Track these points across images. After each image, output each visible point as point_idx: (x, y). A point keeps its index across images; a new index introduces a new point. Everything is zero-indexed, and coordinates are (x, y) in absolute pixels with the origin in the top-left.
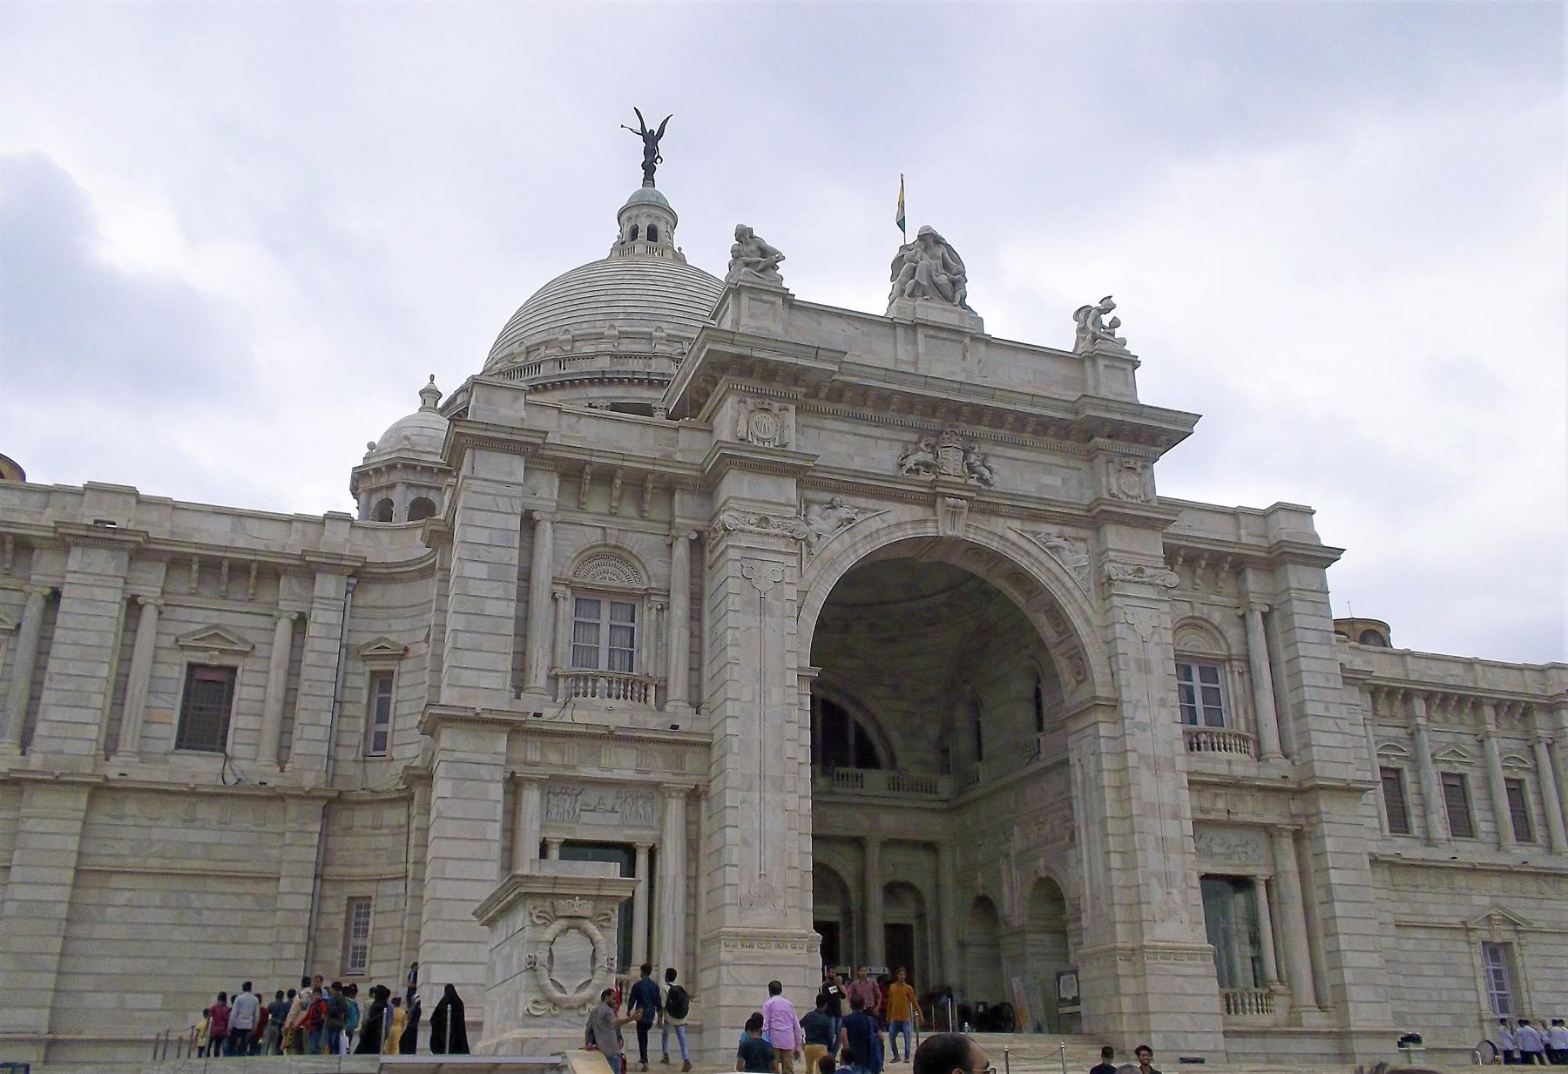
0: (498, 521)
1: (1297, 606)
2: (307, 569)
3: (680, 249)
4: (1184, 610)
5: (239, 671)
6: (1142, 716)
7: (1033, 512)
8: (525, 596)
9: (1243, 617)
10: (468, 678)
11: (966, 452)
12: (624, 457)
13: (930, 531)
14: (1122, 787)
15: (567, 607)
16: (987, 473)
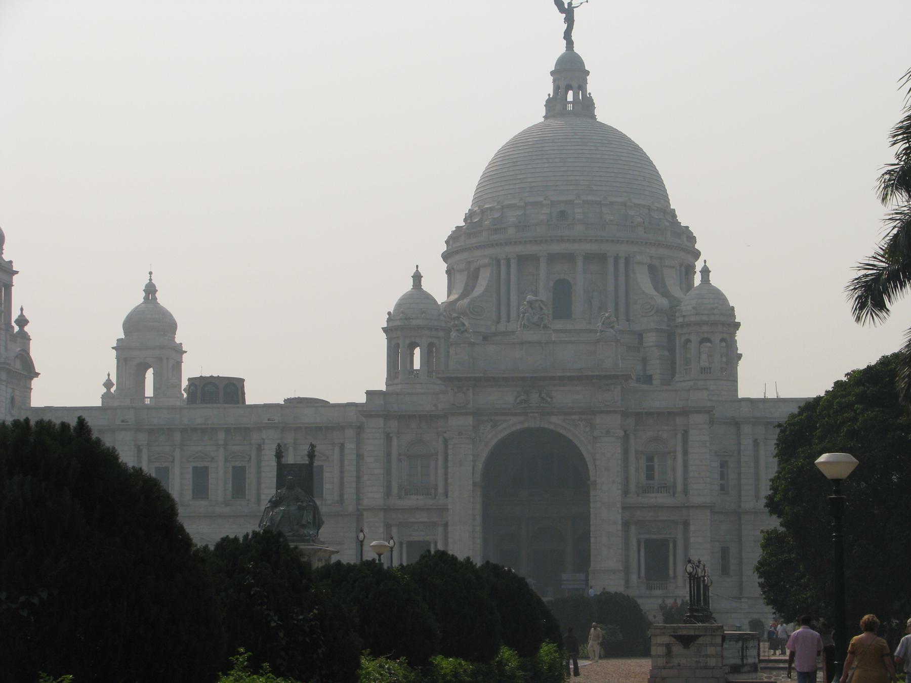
1: (691, 432)
3: (590, 94)
5: (324, 467)
8: (389, 461)
13: (526, 425)
16: (549, 400)
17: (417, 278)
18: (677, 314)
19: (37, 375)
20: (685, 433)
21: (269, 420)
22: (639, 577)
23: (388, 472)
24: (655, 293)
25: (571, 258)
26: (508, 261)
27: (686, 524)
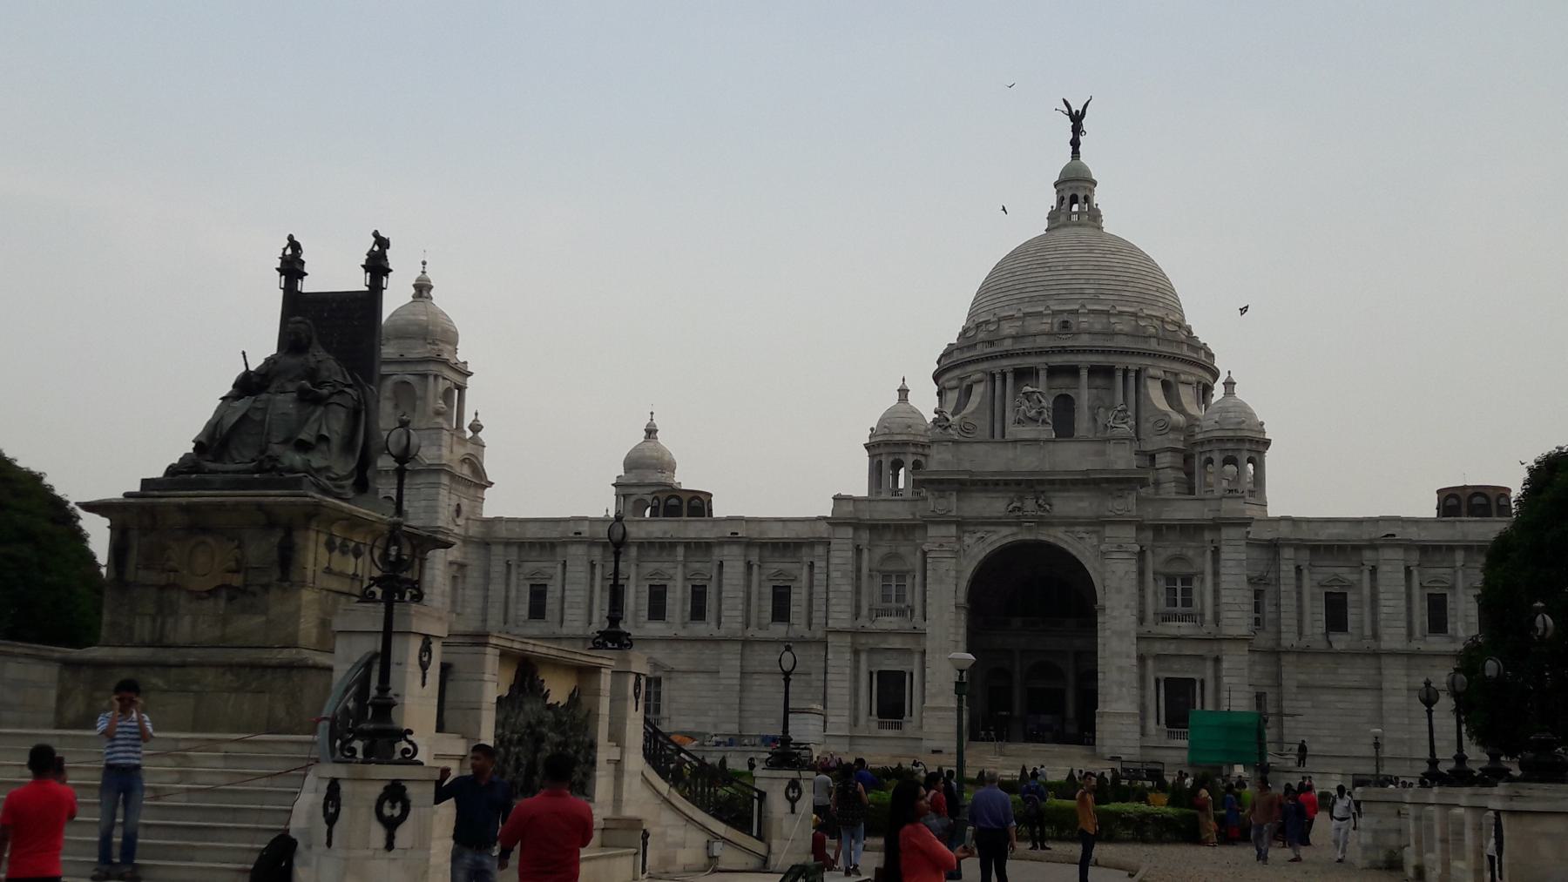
0: (844, 554)
1: (1224, 549)
2: (811, 543)
3: (1097, 205)
4: (1172, 551)
6: (1115, 613)
7: (1070, 523)
8: (858, 578)
9: (1204, 552)
10: (835, 615)
11: (1037, 499)
12: (893, 520)
13: (1020, 537)
14: (1104, 645)
15: (878, 580)
16: (1048, 507)
17: (903, 392)
18: (1197, 430)
19: (493, 483)
20: (1216, 552)
21: (732, 534)
22: (1158, 723)
23: (858, 591)
24: (1171, 410)
25: (1073, 371)
26: (1004, 375)
27: (1217, 660)
